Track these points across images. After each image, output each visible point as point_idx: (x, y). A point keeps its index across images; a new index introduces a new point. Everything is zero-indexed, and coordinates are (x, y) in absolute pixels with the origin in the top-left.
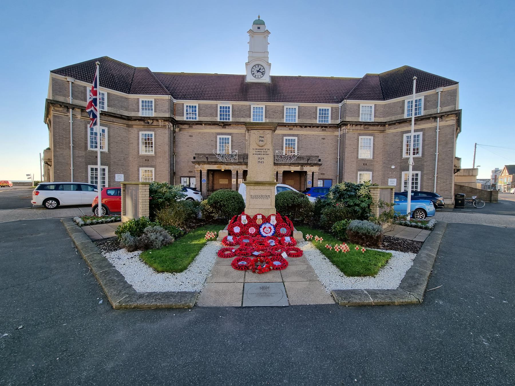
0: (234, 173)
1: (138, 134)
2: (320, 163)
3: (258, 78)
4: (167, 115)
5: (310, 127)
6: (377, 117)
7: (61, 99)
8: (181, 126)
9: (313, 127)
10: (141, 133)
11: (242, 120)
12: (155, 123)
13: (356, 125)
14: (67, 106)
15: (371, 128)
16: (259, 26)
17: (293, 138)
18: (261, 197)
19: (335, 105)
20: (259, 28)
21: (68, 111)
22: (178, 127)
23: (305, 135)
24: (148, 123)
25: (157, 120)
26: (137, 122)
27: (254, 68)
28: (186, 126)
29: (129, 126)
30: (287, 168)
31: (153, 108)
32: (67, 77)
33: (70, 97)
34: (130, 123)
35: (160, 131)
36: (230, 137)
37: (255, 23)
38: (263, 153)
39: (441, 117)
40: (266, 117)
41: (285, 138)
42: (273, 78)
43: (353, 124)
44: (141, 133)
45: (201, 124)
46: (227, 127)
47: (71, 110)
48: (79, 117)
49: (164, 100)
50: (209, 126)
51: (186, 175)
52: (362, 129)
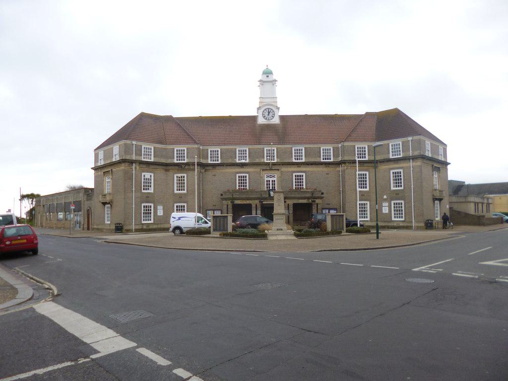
0: (254, 206)
1: (174, 176)
2: (323, 196)
3: (269, 120)
5: (315, 164)
7: (128, 157)
8: (208, 168)
9: (318, 164)
10: (175, 176)
11: (257, 161)
12: (187, 167)
14: (131, 162)
15: (366, 165)
16: (267, 75)
17: (301, 174)
18: (280, 219)
19: (336, 145)
20: (267, 76)
22: (204, 168)
23: (312, 172)
25: (189, 165)
26: (173, 167)
29: (167, 170)
30: (296, 201)
31: (186, 155)
33: (134, 155)
36: (247, 175)
37: (264, 73)
39: (413, 159)
40: (277, 157)
41: (294, 174)
42: (282, 118)
43: (350, 163)
44: (175, 176)
46: (244, 167)
48: (138, 168)
49: (193, 148)
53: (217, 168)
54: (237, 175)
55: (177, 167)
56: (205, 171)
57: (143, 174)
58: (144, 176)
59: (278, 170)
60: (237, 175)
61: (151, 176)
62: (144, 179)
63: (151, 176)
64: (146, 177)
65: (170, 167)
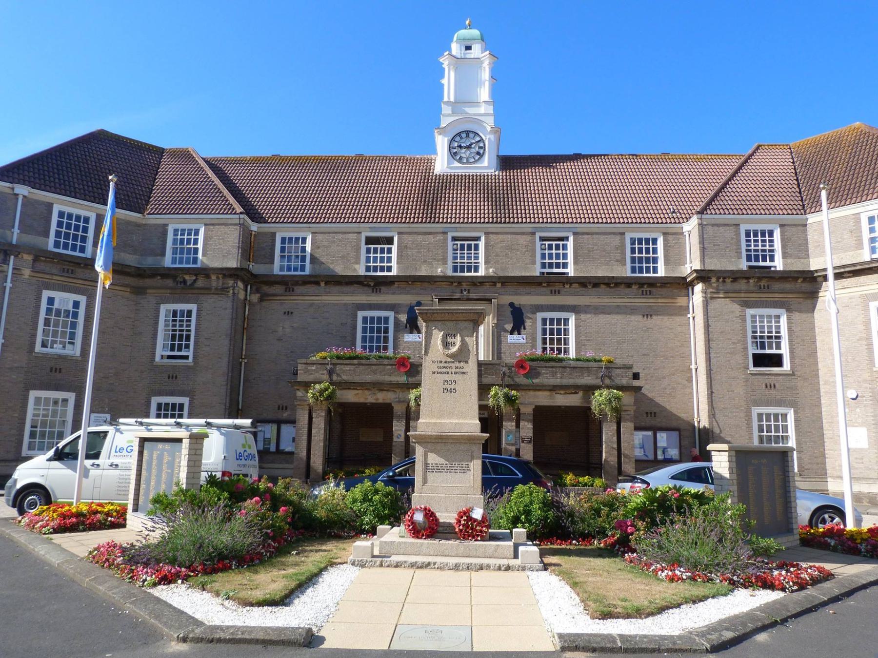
2: (636, 383)
3: (468, 162)
4: (233, 263)
5: (608, 285)
6: (791, 256)
8: (265, 289)
9: (617, 285)
10: (164, 308)
13: (735, 280)
16: (468, 43)
17: (562, 315)
21: (6, 261)
22: (258, 291)
24: (185, 282)
26: (158, 281)
27: (458, 139)
28: (278, 289)
30: (544, 399)
32: (16, 185)
33: (16, 230)
34: (141, 283)
35: (210, 302)
38: (454, 370)
44: (164, 308)
45: (317, 283)
46: (383, 289)
47: (12, 257)
48: (27, 272)
50: (338, 288)
51: (270, 416)
52: (752, 288)
53: (299, 289)
54: (361, 314)
55: (169, 282)
56: (261, 300)
57: (46, 294)
58: (51, 301)
59: (490, 300)
60: (361, 314)
61: (76, 304)
62: (49, 311)
63: (76, 304)
64: (56, 305)
65: (148, 282)
